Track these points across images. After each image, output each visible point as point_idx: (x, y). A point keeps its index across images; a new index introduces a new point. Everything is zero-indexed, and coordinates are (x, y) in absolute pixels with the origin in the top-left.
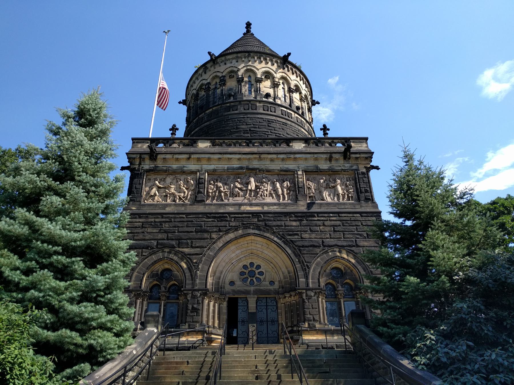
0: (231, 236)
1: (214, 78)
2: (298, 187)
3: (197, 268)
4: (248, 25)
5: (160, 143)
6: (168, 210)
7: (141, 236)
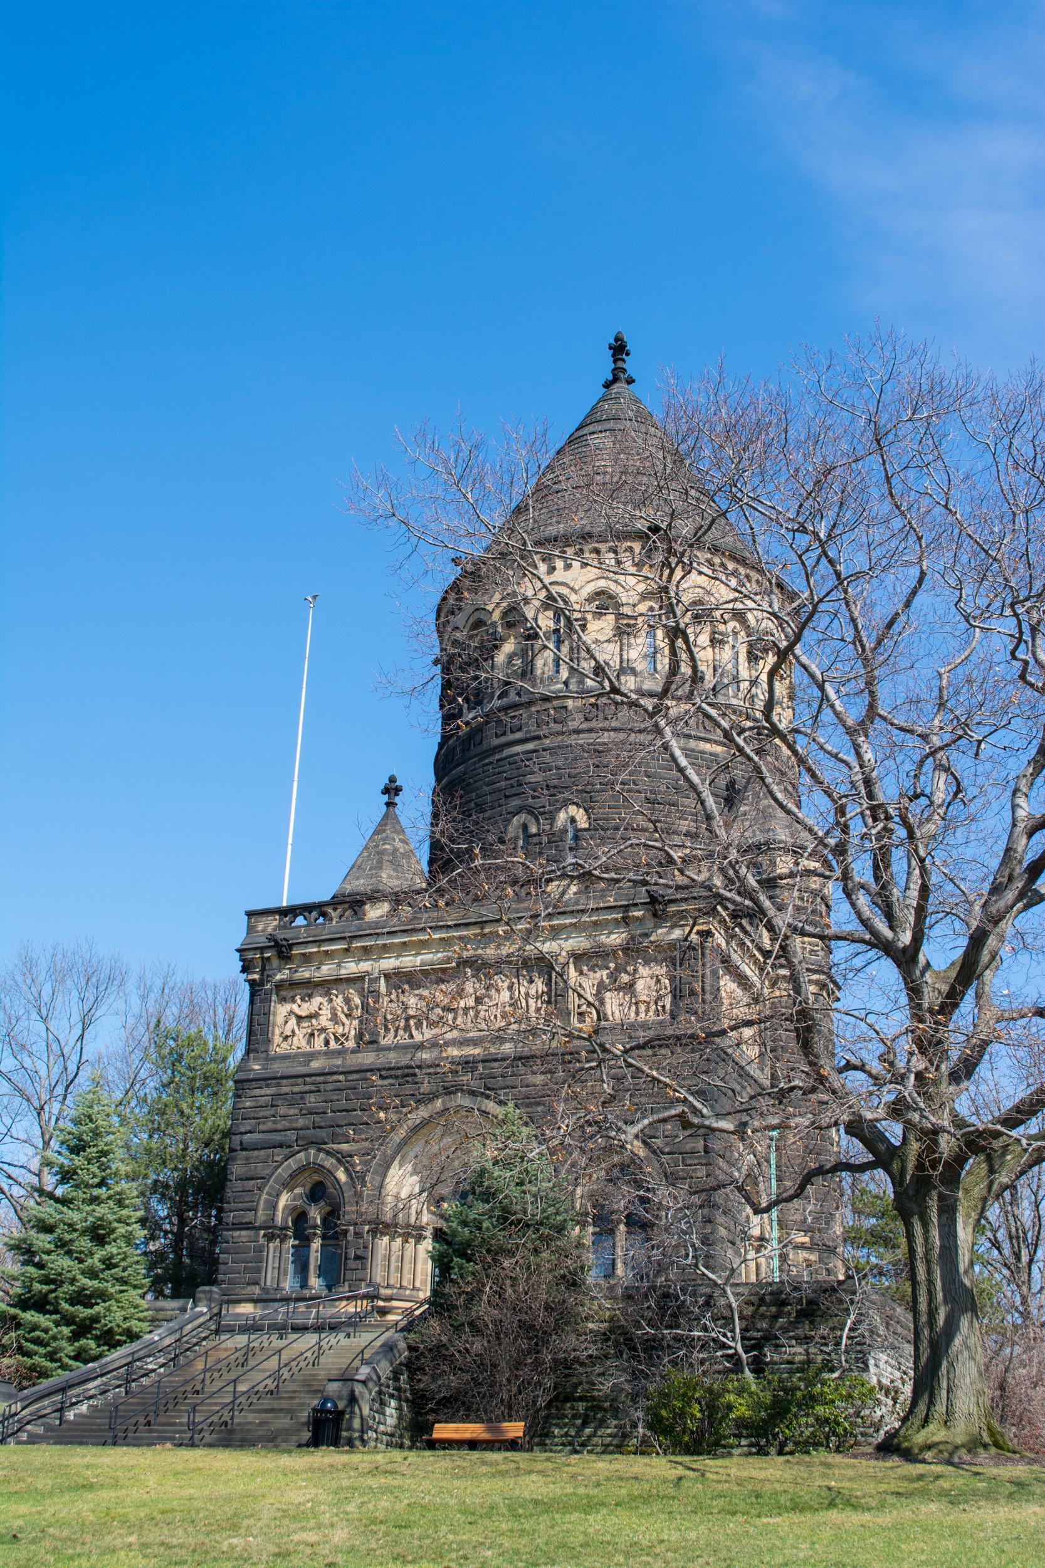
0: (424, 1112)
2: (556, 995)
3: (364, 1184)
4: (619, 349)
5: (295, 916)
6: (315, 1065)
7: (269, 1125)
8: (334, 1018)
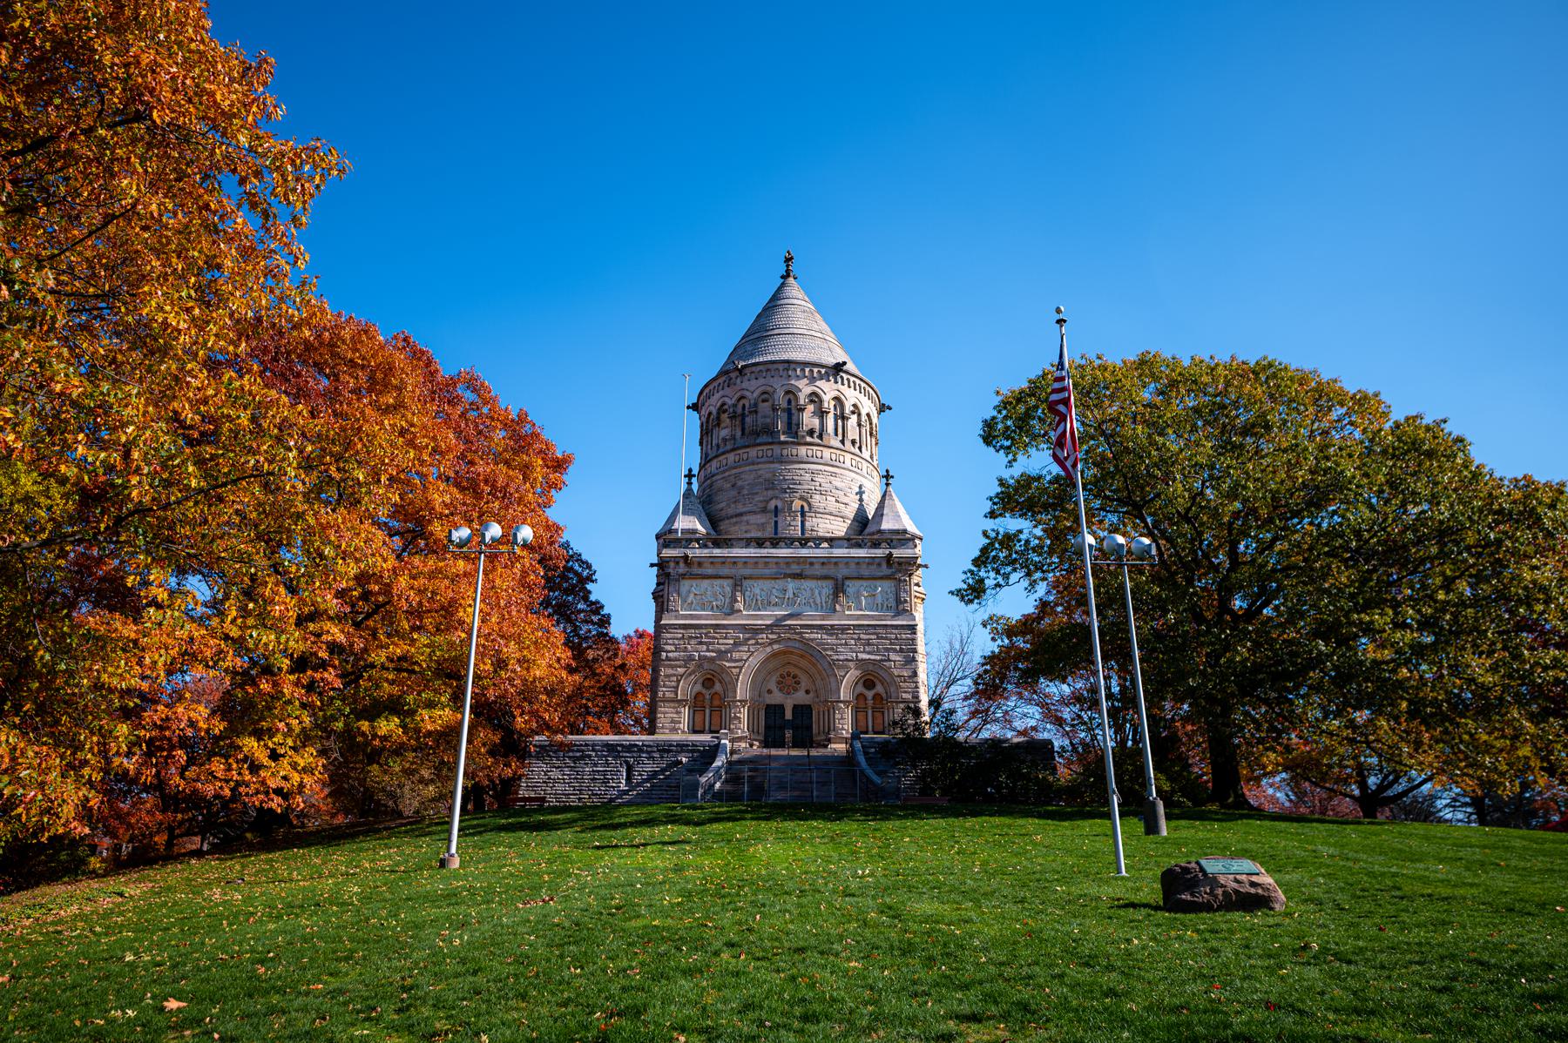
1: (742, 397)
4: (788, 260)
8: (715, 595)
